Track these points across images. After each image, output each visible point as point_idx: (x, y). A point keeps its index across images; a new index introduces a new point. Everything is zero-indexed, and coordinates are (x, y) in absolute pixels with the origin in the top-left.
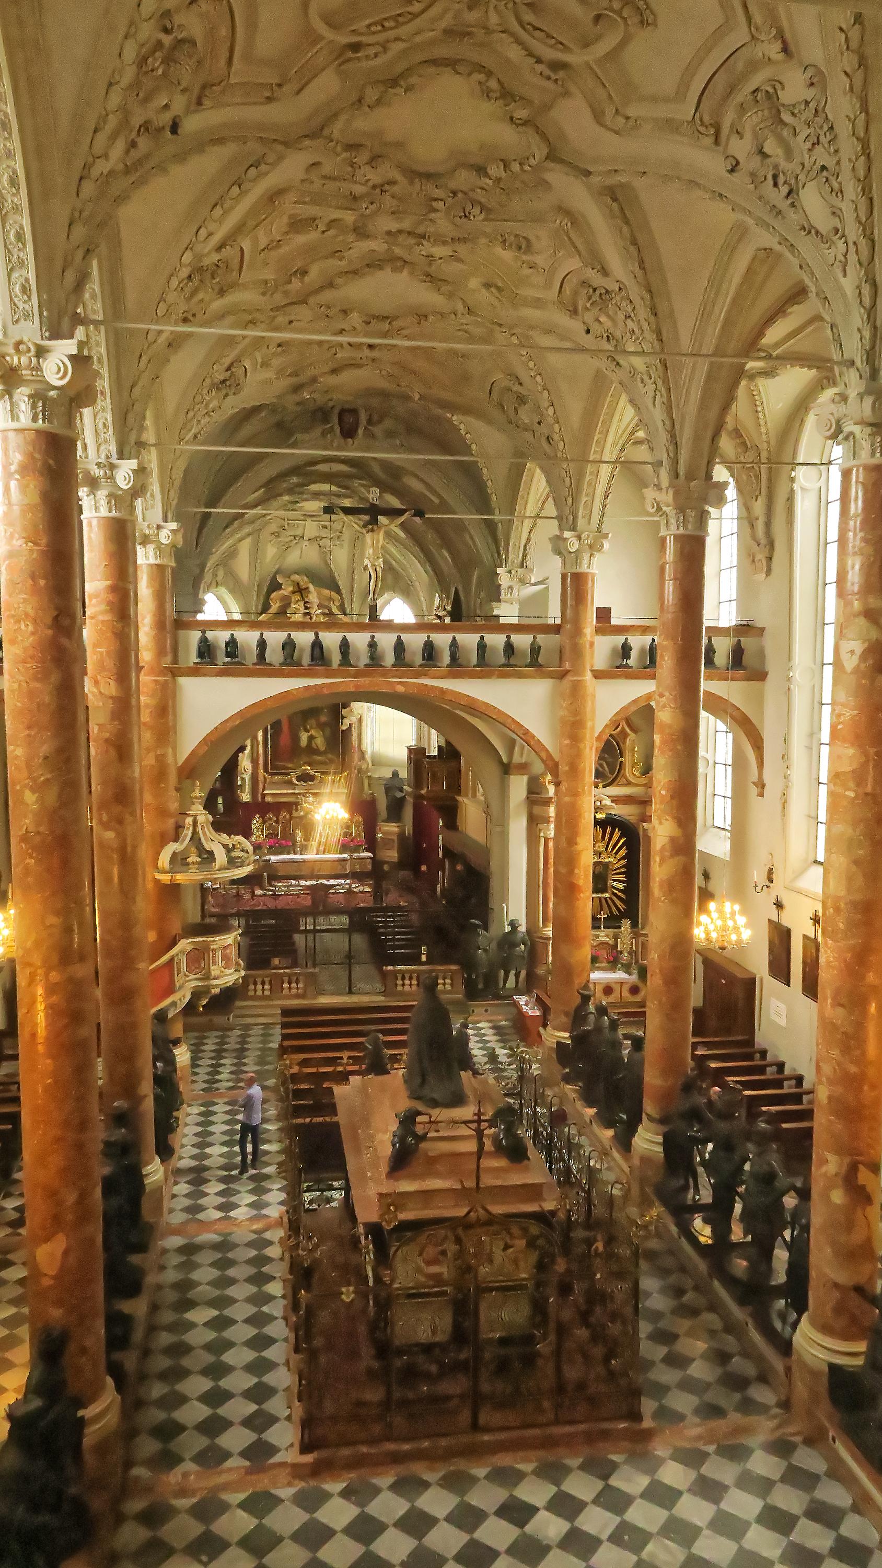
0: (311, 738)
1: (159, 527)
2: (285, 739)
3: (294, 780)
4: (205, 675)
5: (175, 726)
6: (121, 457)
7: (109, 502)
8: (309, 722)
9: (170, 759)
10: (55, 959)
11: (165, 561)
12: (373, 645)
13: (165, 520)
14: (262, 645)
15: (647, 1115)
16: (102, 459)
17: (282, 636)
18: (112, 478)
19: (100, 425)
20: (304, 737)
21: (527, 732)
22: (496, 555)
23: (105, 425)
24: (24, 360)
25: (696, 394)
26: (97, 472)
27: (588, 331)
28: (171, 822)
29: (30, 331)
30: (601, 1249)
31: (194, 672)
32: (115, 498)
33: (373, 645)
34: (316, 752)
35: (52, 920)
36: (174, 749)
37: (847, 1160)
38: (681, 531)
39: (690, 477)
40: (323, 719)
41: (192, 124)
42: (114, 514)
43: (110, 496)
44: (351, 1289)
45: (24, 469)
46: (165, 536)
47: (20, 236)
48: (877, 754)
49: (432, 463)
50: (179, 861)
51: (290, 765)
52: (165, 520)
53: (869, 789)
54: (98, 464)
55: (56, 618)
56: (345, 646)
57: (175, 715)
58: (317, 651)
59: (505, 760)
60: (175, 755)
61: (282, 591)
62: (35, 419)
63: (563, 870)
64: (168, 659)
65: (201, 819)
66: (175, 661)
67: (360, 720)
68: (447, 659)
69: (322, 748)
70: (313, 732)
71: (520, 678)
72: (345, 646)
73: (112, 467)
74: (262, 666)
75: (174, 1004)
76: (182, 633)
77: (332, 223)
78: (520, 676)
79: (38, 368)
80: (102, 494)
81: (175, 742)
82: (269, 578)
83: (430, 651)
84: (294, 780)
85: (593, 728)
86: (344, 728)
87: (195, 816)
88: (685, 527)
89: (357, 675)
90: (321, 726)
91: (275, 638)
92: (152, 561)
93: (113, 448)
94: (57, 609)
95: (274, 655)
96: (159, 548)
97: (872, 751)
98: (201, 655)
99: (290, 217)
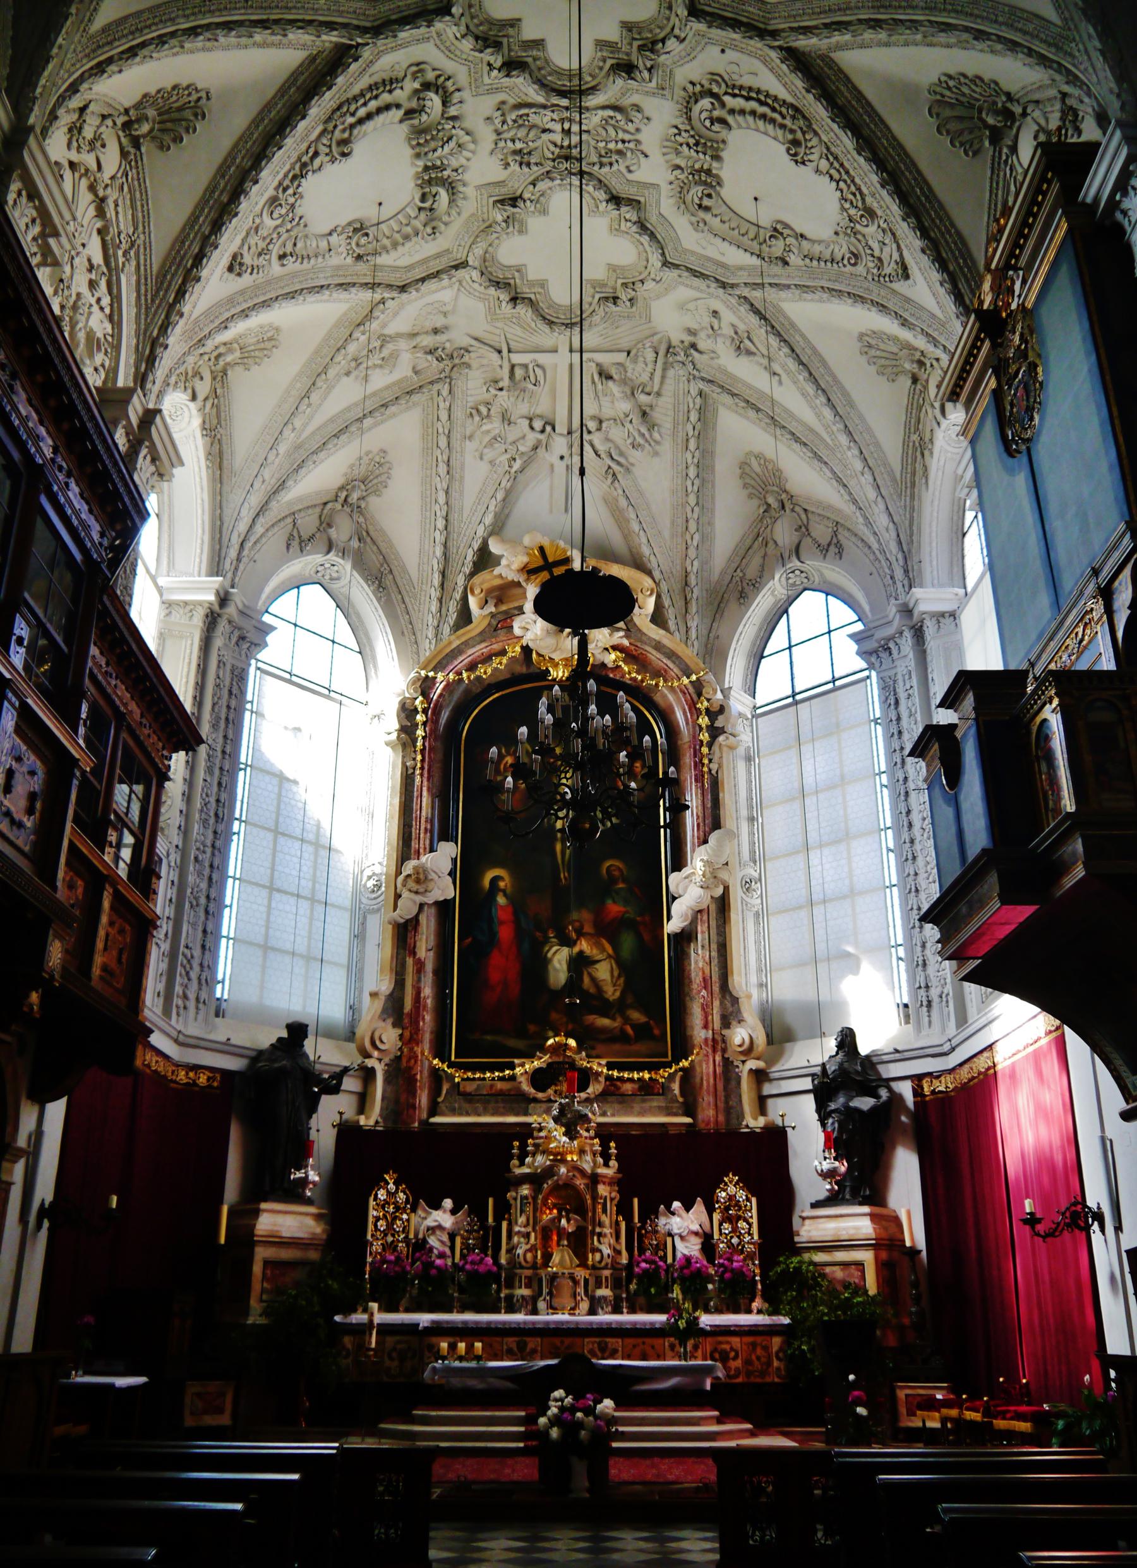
2: (501, 967)
3: (526, 1087)
8: (575, 916)
20: (559, 959)
40: (614, 908)
51: (513, 1043)
61: (497, 571)
67: (723, 904)
82: (470, 553)
84: (526, 1087)
86: (672, 926)
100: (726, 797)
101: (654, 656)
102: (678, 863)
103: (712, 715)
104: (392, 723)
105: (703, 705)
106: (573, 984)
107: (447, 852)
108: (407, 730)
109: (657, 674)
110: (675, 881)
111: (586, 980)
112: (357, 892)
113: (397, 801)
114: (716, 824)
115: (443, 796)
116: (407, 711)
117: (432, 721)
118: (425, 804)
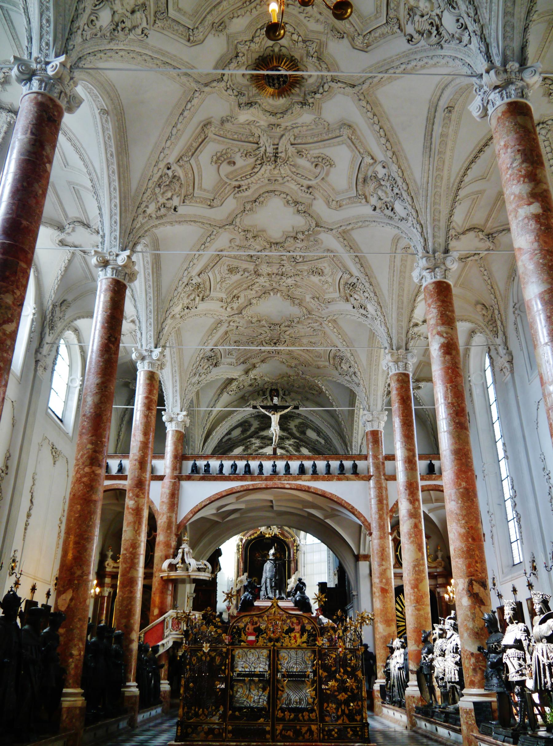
1: (178, 414)
4: (193, 480)
5: (177, 504)
6: (156, 347)
9: (174, 520)
10: (88, 462)
11: (180, 429)
12: (274, 466)
13: (181, 411)
14: (222, 466)
15: (411, 671)
16: (148, 348)
17: (232, 462)
18: (151, 356)
21: (353, 508)
24: (111, 258)
25: (394, 315)
26: (145, 353)
27: (354, 308)
28: (172, 551)
29: (116, 250)
30: (341, 634)
31: (189, 478)
32: (152, 364)
33: (274, 466)
35: (89, 446)
36: (176, 514)
37: (467, 580)
38: (397, 371)
39: (398, 349)
41: (181, 210)
42: (150, 369)
43: (149, 363)
44: (208, 645)
45: (106, 290)
46: (180, 418)
47: (115, 222)
48: (451, 386)
49: (314, 411)
50: (172, 567)
52: (181, 411)
53: (450, 401)
54: (146, 350)
55: (109, 337)
56: (261, 466)
57: (178, 498)
58: (247, 469)
59: (356, 553)
60: (176, 519)
62: (112, 275)
64: (178, 472)
65: (186, 550)
66: (180, 473)
68: (311, 471)
72: (261, 466)
73: (151, 352)
74: (220, 476)
75: (163, 645)
76: (184, 462)
77: (245, 270)
78: (348, 479)
79: (116, 260)
80: (146, 362)
81: (177, 511)
83: (302, 470)
85: (387, 505)
87: (184, 549)
88: (399, 370)
89: (267, 479)
91: (227, 464)
92: (174, 429)
93: (153, 345)
94: (110, 334)
95: (227, 470)
96: (178, 423)
97: (448, 385)
98: (193, 471)
99: (228, 266)
100: (299, 564)
101: (286, 534)
102: (289, 577)
103: (297, 546)
104: (235, 549)
105: (295, 544)
107: (246, 574)
108: (238, 550)
109: (287, 538)
110: (289, 581)
112: (228, 581)
113: (236, 564)
114: (297, 570)
115: (245, 563)
116: (238, 546)
117: (243, 548)
118: (242, 565)
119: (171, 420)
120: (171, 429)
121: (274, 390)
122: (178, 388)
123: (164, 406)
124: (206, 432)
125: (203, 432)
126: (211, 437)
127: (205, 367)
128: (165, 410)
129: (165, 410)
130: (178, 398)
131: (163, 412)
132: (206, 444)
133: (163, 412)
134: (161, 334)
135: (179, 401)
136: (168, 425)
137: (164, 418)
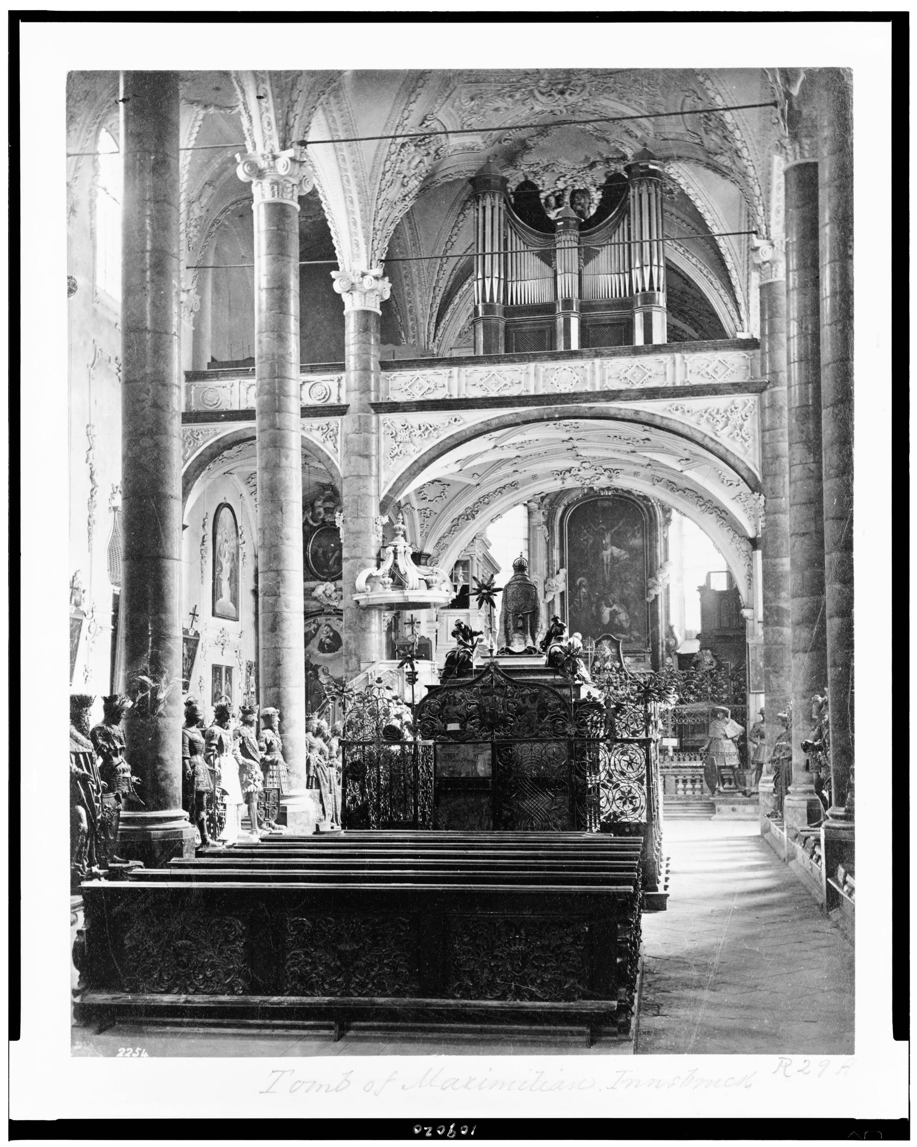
0: (614, 614)
7: (273, 188)
16: (266, 152)
19: (265, 124)
20: (606, 611)
22: (737, 320)
23: (269, 124)
26: (263, 164)
34: (620, 629)
54: (263, 156)
63: (770, 595)
69: (626, 625)
70: (615, 607)
71: (716, 394)
86: (649, 600)
88: (802, 155)
90: (624, 602)
93: (276, 143)
106: (611, 621)
111: (617, 620)
119: (352, 289)
120: (352, 305)
121: (579, 190)
122: (358, 216)
123: (336, 259)
124: (438, 300)
125: (434, 298)
126: (451, 307)
127: (414, 163)
128: (336, 268)
129: (336, 268)
130: (361, 240)
131: (333, 274)
132: (442, 325)
133: (333, 274)
134: (292, 115)
135: (363, 247)
136: (346, 298)
137: (337, 287)
